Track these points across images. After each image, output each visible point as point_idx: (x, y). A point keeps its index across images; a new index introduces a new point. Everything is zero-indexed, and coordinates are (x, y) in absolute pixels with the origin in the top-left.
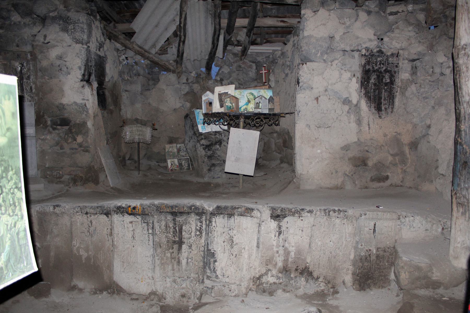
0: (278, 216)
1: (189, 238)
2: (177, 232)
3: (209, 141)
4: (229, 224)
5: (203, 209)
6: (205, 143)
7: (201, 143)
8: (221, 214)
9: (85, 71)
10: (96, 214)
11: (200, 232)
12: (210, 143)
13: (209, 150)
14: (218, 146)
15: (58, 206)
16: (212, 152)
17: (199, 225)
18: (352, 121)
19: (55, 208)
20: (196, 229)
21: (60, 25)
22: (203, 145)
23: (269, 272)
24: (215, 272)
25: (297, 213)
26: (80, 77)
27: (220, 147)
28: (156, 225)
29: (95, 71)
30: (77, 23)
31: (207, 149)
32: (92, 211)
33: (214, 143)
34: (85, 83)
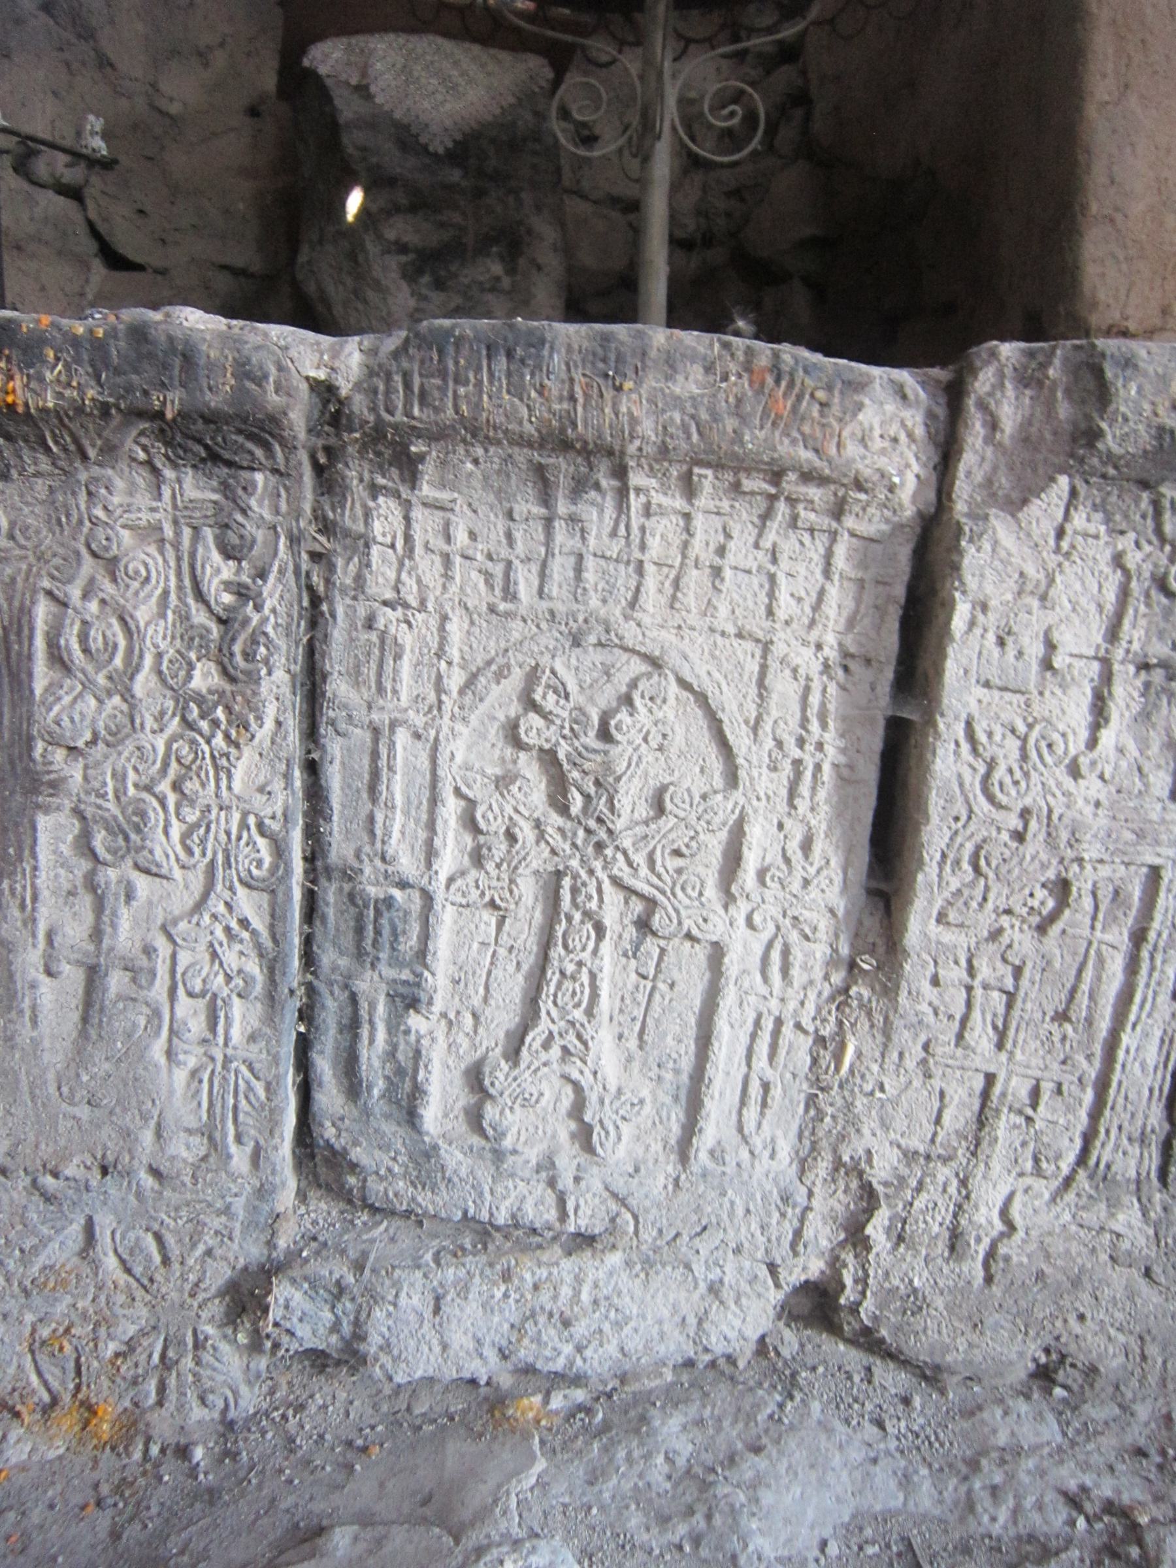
1: (115, 738)
3: (442, 225)
4: (561, 568)
6: (411, 238)
7: (391, 235)
8: (475, 431)
11: (225, 672)
14: (497, 268)
17: (213, 587)
20: (189, 635)
22: (403, 248)
23: (1004, 1127)
24: (412, 1118)
27: (511, 271)
33: (469, 239)
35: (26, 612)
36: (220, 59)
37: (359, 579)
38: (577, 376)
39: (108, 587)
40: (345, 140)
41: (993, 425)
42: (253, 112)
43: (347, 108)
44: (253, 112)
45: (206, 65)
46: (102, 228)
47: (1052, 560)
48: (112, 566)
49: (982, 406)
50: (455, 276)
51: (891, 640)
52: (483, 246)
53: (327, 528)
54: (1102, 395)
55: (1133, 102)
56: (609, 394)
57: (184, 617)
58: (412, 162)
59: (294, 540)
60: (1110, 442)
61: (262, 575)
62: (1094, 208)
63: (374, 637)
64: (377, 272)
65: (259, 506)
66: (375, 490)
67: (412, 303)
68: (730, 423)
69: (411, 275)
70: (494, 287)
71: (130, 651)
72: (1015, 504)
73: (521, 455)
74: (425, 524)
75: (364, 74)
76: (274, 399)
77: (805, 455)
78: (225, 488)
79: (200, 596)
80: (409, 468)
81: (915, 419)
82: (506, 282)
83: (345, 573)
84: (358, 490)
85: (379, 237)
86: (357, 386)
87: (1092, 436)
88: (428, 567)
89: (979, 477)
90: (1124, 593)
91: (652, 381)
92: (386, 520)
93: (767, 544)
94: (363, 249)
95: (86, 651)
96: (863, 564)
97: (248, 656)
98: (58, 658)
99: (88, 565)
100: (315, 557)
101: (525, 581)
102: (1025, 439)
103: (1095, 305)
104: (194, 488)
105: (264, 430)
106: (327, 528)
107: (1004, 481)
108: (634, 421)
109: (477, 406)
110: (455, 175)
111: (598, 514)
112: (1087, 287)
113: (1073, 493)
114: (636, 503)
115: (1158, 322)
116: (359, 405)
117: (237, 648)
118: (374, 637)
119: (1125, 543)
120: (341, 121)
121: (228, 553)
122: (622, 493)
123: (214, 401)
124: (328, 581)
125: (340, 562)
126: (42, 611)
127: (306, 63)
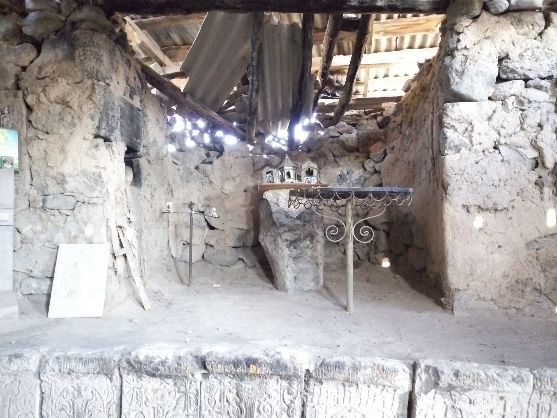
0: (450, 388)
2: (241, 412)
3: (296, 234)
4: (347, 399)
5: (295, 369)
6: (289, 238)
7: (284, 238)
8: (333, 379)
9: (100, 121)
10: (89, 373)
12: (297, 237)
13: (295, 248)
15: (17, 356)
16: (299, 251)
18: (546, 196)
19: (10, 360)
20: (282, 409)
21: (63, 50)
22: (287, 241)
25: (493, 384)
26: (94, 131)
27: (312, 243)
28: (204, 395)
29: (122, 126)
30: (90, 46)
31: (292, 247)
32: (81, 367)
33: (302, 237)
34: (101, 141)
35: (254, 403)
36: (238, 179)
37: (312, 400)
38: (350, 372)
39: (268, 400)
40: (274, 216)
41: (421, 379)
42: (245, 191)
43: (274, 208)
44: (245, 191)
45: (234, 181)
46: (208, 220)
47: (433, 402)
48: (269, 396)
49: (419, 375)
50: (299, 246)
51: (406, 412)
52: (305, 238)
53: (307, 391)
54: (439, 377)
55: (456, 241)
56: (355, 374)
57: (281, 405)
58: (289, 220)
59: (301, 393)
60: (441, 385)
61: (295, 398)
62: (449, 263)
63: (314, 409)
64: (281, 246)
65: (295, 386)
66: (315, 385)
67: (289, 253)
68: (376, 379)
69: (288, 247)
70: (308, 247)
71: (272, 411)
72: (426, 393)
73: (340, 382)
74: (323, 391)
75: (278, 200)
76: (300, 374)
77: (389, 384)
78: (289, 384)
79: (284, 401)
80: (321, 383)
81: (408, 376)
82: (311, 246)
83: (309, 398)
84: (312, 385)
85: (281, 238)
86: (313, 371)
87: (438, 384)
88: (323, 397)
89: (419, 386)
90: (447, 409)
91: (362, 371)
92: (317, 389)
93: (383, 395)
94: (277, 240)
95: (264, 410)
96: (400, 399)
97: (292, 412)
98: (259, 411)
99: (265, 396)
100: (305, 395)
101: (341, 400)
102: (426, 381)
103: (452, 284)
104: (285, 383)
105: (297, 377)
106: (307, 391)
107: (424, 388)
108: (360, 378)
109: (334, 376)
110: (298, 222)
111: (353, 389)
112: (449, 280)
113: (436, 392)
114: (360, 388)
115: (466, 288)
116: (314, 374)
117: (290, 411)
118: (314, 409)
119: (446, 400)
120: (273, 211)
121: (289, 394)
122: (358, 387)
123: (290, 374)
124: (307, 400)
125: (308, 397)
126: (257, 403)
127: (264, 197)
